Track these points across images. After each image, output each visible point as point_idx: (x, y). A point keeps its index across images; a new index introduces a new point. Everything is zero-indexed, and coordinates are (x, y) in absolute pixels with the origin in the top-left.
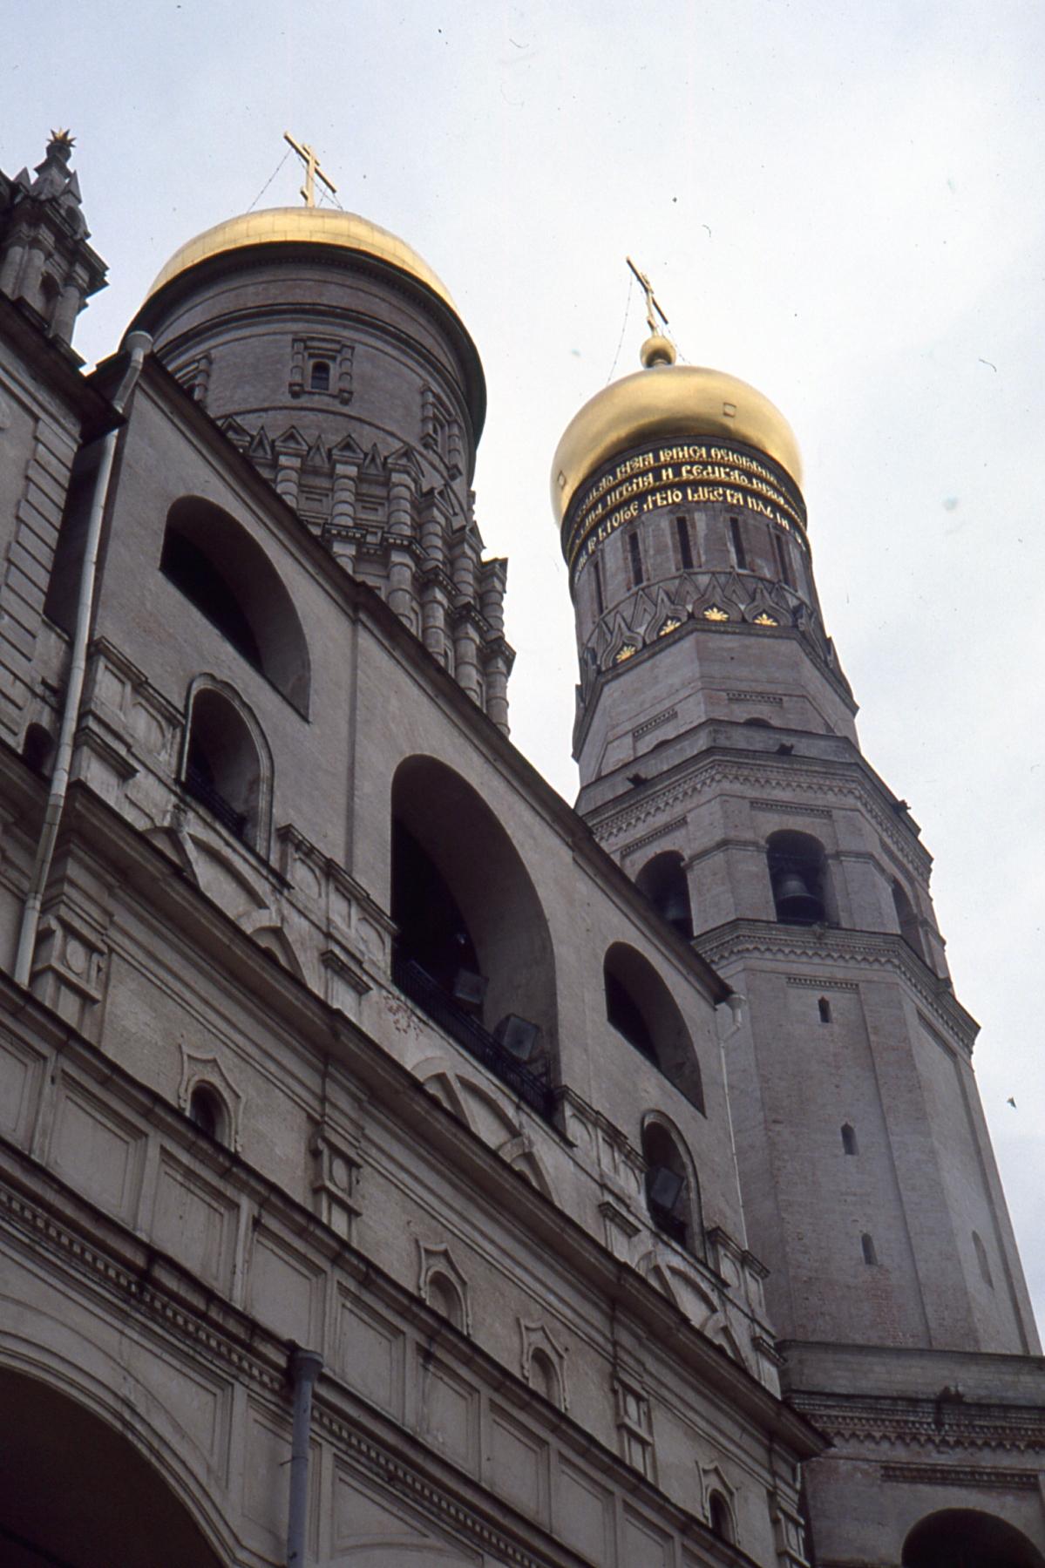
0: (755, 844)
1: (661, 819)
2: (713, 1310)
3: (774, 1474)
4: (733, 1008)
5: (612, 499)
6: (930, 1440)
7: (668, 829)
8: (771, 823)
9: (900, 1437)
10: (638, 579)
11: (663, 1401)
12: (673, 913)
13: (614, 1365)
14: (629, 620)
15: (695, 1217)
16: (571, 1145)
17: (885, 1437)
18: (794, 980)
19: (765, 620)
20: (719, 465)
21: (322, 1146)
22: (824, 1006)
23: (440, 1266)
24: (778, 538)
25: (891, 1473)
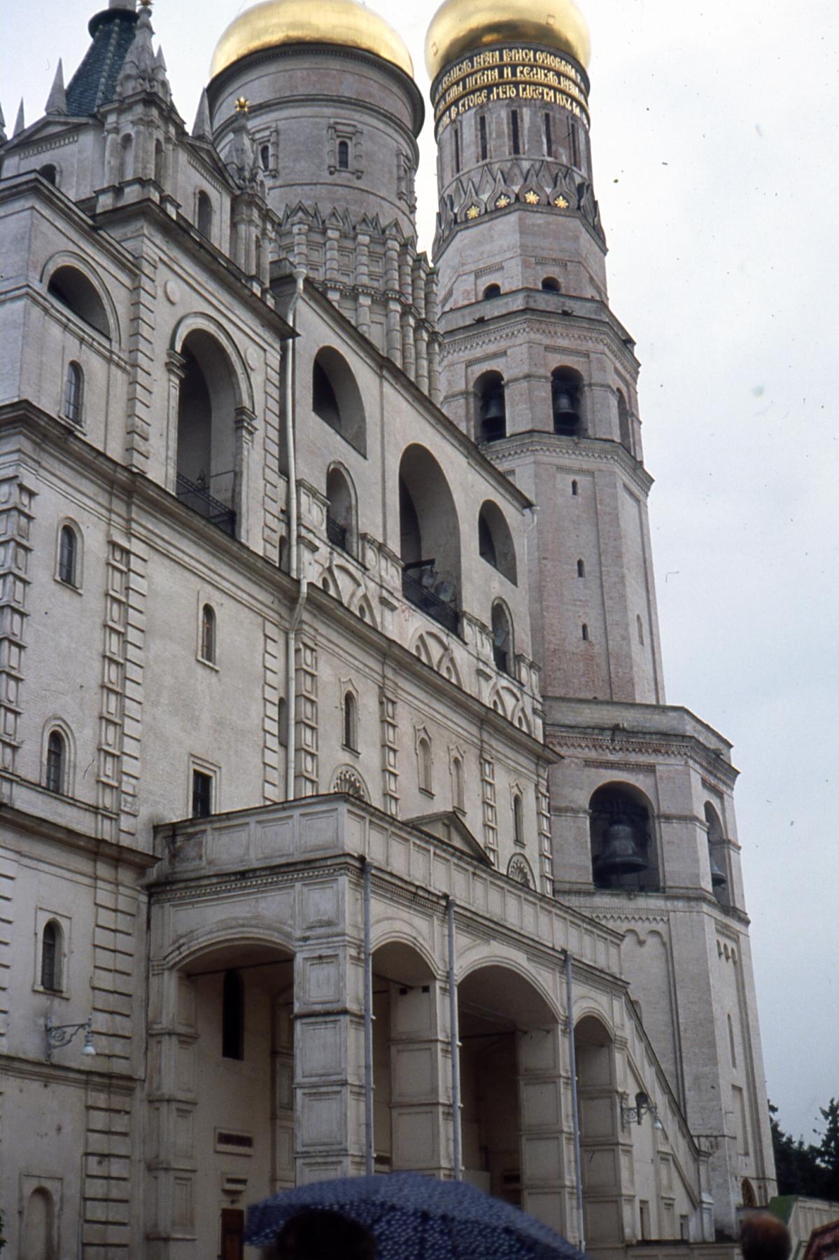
0: (546, 378)
1: (491, 348)
2: (518, 700)
3: (538, 776)
4: (533, 513)
5: (470, 82)
6: (608, 747)
7: (495, 356)
8: (556, 361)
9: (594, 746)
10: (484, 157)
11: (498, 759)
12: (493, 413)
13: (481, 751)
14: (477, 186)
15: (511, 649)
16: (466, 644)
18: (560, 468)
19: (561, 203)
20: (541, 67)
21: (384, 700)
22: (574, 484)
23: (423, 735)
24: (573, 126)
25: (588, 763)
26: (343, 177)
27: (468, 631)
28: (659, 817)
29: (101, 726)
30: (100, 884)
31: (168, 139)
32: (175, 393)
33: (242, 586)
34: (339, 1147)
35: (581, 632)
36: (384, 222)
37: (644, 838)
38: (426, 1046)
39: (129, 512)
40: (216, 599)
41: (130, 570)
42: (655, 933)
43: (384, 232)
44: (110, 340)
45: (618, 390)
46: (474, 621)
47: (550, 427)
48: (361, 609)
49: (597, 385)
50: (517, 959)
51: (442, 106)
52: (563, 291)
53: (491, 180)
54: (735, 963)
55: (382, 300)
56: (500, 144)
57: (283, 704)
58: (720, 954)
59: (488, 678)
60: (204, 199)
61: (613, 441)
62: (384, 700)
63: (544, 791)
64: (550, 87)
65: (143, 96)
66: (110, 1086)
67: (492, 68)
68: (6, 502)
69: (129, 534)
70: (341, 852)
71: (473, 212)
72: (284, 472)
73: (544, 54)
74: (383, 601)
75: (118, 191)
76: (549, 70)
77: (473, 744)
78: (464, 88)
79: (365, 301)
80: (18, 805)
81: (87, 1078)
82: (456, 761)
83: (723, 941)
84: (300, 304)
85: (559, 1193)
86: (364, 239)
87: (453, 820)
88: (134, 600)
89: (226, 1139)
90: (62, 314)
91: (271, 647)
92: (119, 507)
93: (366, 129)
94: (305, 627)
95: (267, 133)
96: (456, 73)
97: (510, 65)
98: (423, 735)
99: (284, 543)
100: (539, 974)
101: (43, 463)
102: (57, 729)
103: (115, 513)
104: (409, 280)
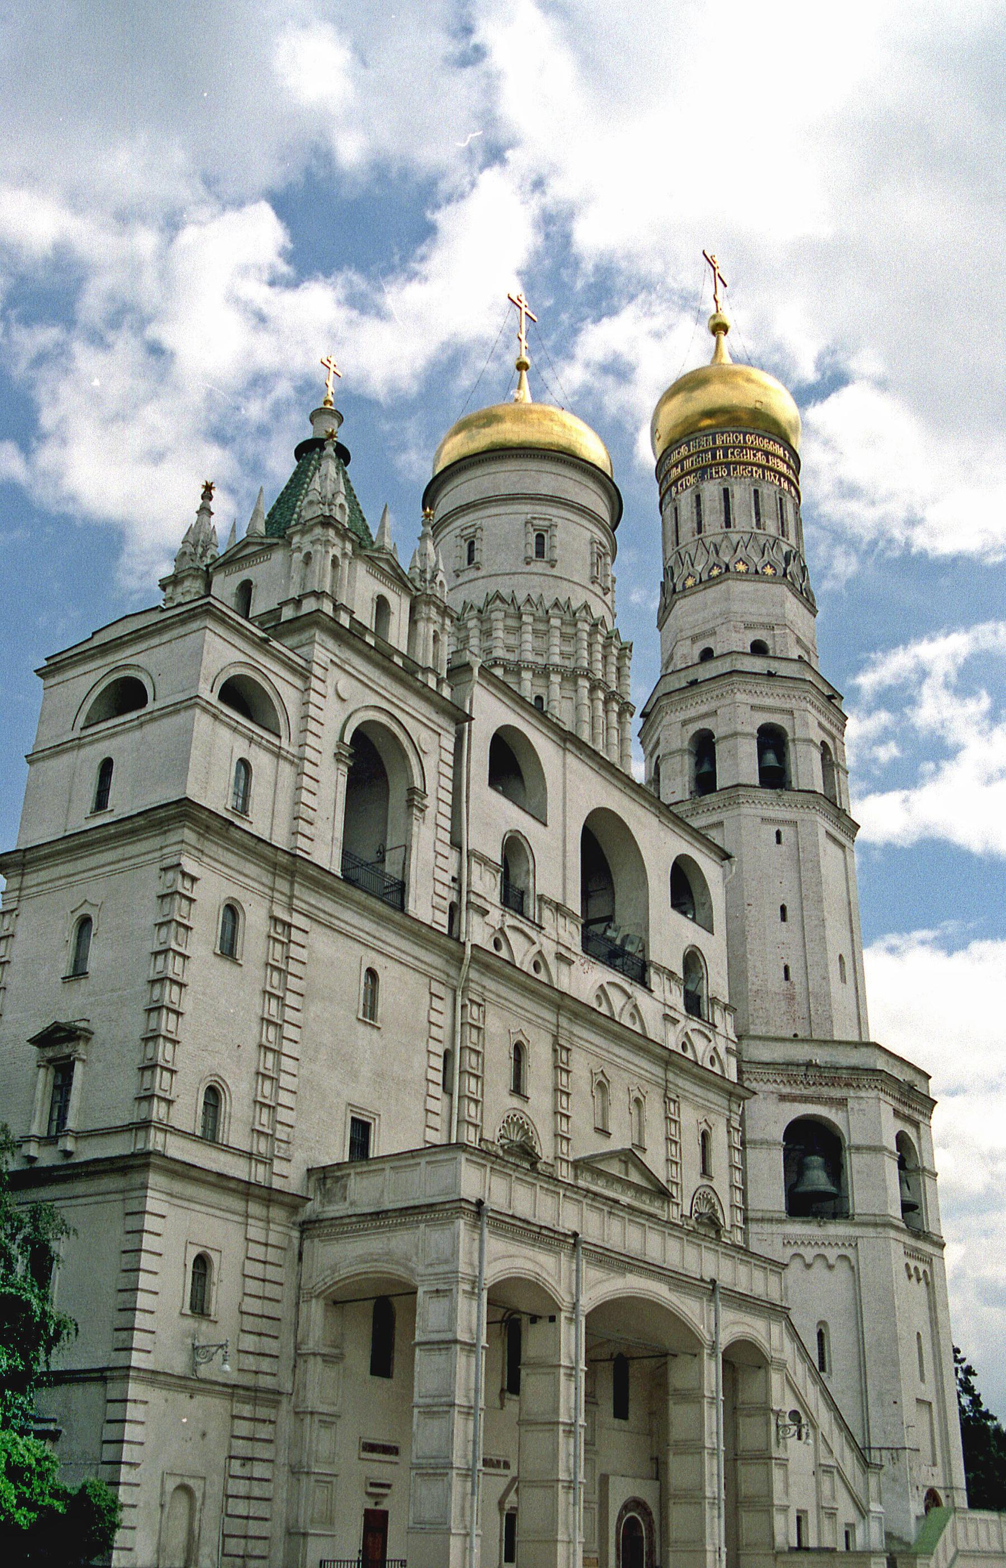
0: (751, 735)
1: (703, 709)
3: (730, 1111)
6: (802, 1082)
8: (762, 719)
10: (700, 532)
11: (685, 1098)
12: (706, 768)
15: (705, 992)
16: (651, 991)
17: (782, 1081)
18: (764, 820)
19: (769, 571)
20: (750, 448)
21: (558, 1048)
22: (778, 834)
23: (600, 1078)
24: (781, 499)
25: (783, 1098)
26: (539, 567)
27: (655, 979)
28: (850, 1148)
29: (257, 1082)
30: (250, 1221)
31: (345, 555)
32: (343, 781)
33: (408, 951)
34: (447, 1460)
35: (783, 973)
36: (575, 605)
37: (836, 1170)
38: (553, 1370)
39: (292, 889)
40: (378, 963)
41: (290, 941)
42: (843, 1257)
43: (575, 614)
44: (280, 737)
45: (823, 743)
46: (661, 970)
47: (756, 780)
48: (536, 966)
49: (799, 740)
50: (659, 1290)
51: (665, 486)
52: (771, 653)
53: (705, 552)
54: (927, 1284)
55: (571, 677)
56: (713, 520)
57: (448, 1056)
58: (910, 1277)
59: (675, 1022)
60: (382, 604)
61: (814, 792)
62: (557, 1047)
63: (736, 1125)
64: (759, 466)
65: (321, 518)
66: (256, 1398)
67: (706, 451)
68: (170, 887)
69: (291, 909)
70: (456, 1198)
71: (690, 582)
72: (456, 844)
73: (753, 436)
74: (560, 957)
75: (298, 602)
76: (758, 450)
77: (658, 1085)
78: (682, 469)
79: (555, 678)
80: (171, 1153)
81: (232, 1390)
82: (637, 1101)
83: (913, 1263)
84: (477, 690)
85: (700, 1503)
86: (555, 622)
87: (630, 1157)
88: (293, 967)
89: (370, 1448)
90: (231, 718)
91: (437, 1004)
92: (282, 885)
93: (559, 521)
94: (472, 985)
95: (472, 530)
96: (675, 457)
97: (722, 448)
98: (600, 1078)
99: (454, 909)
100: (682, 1302)
101: (206, 851)
102: (213, 1083)
103: (278, 891)
104: (599, 657)
